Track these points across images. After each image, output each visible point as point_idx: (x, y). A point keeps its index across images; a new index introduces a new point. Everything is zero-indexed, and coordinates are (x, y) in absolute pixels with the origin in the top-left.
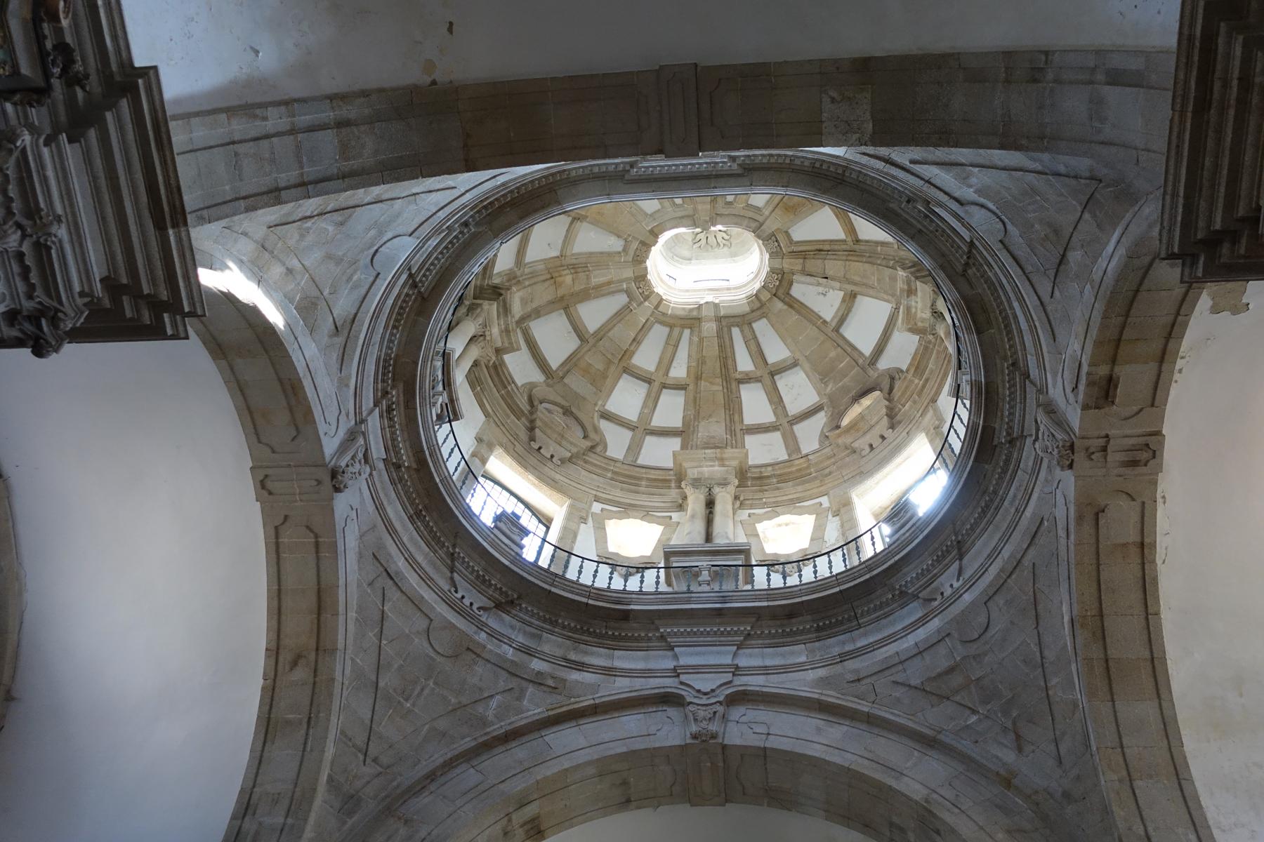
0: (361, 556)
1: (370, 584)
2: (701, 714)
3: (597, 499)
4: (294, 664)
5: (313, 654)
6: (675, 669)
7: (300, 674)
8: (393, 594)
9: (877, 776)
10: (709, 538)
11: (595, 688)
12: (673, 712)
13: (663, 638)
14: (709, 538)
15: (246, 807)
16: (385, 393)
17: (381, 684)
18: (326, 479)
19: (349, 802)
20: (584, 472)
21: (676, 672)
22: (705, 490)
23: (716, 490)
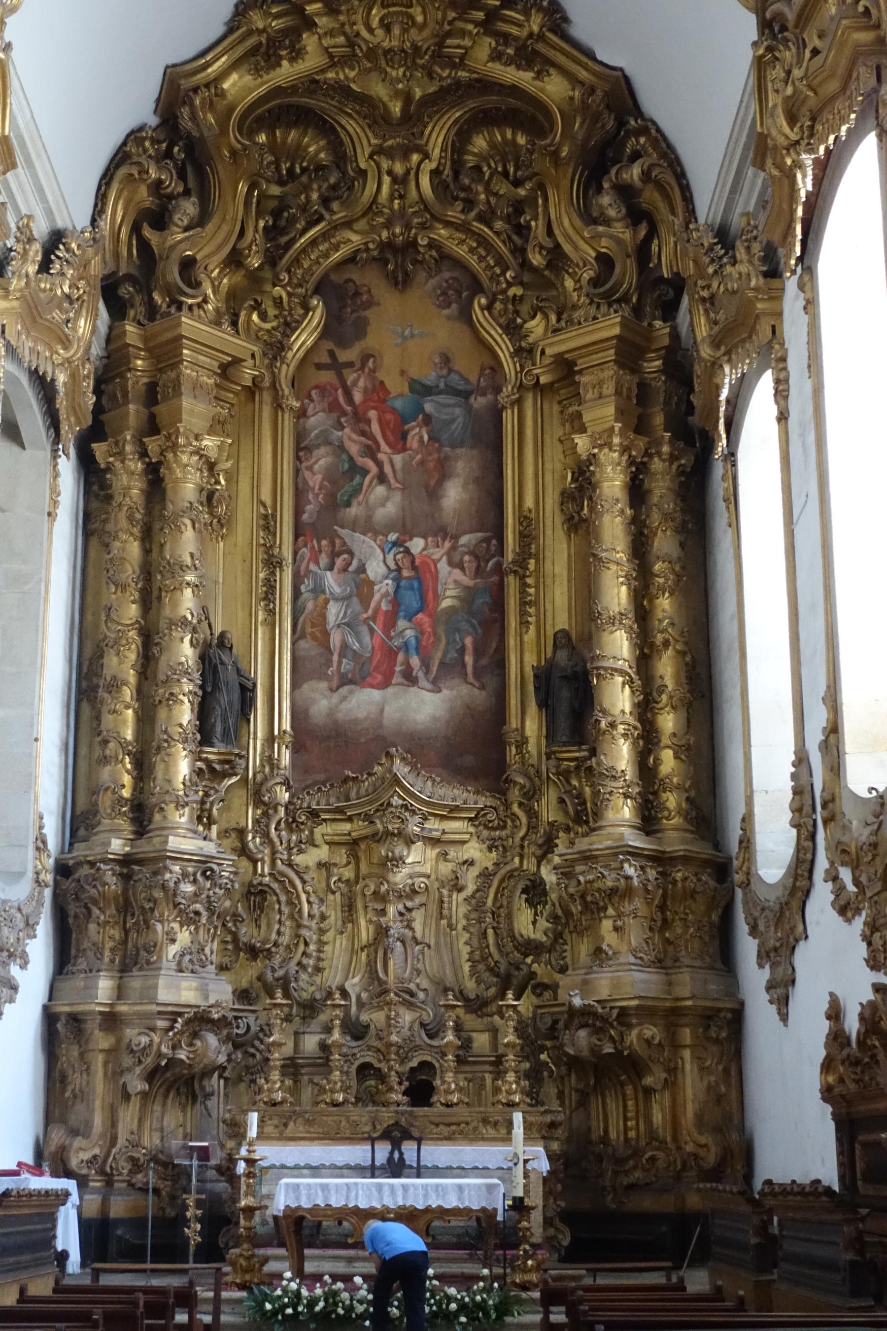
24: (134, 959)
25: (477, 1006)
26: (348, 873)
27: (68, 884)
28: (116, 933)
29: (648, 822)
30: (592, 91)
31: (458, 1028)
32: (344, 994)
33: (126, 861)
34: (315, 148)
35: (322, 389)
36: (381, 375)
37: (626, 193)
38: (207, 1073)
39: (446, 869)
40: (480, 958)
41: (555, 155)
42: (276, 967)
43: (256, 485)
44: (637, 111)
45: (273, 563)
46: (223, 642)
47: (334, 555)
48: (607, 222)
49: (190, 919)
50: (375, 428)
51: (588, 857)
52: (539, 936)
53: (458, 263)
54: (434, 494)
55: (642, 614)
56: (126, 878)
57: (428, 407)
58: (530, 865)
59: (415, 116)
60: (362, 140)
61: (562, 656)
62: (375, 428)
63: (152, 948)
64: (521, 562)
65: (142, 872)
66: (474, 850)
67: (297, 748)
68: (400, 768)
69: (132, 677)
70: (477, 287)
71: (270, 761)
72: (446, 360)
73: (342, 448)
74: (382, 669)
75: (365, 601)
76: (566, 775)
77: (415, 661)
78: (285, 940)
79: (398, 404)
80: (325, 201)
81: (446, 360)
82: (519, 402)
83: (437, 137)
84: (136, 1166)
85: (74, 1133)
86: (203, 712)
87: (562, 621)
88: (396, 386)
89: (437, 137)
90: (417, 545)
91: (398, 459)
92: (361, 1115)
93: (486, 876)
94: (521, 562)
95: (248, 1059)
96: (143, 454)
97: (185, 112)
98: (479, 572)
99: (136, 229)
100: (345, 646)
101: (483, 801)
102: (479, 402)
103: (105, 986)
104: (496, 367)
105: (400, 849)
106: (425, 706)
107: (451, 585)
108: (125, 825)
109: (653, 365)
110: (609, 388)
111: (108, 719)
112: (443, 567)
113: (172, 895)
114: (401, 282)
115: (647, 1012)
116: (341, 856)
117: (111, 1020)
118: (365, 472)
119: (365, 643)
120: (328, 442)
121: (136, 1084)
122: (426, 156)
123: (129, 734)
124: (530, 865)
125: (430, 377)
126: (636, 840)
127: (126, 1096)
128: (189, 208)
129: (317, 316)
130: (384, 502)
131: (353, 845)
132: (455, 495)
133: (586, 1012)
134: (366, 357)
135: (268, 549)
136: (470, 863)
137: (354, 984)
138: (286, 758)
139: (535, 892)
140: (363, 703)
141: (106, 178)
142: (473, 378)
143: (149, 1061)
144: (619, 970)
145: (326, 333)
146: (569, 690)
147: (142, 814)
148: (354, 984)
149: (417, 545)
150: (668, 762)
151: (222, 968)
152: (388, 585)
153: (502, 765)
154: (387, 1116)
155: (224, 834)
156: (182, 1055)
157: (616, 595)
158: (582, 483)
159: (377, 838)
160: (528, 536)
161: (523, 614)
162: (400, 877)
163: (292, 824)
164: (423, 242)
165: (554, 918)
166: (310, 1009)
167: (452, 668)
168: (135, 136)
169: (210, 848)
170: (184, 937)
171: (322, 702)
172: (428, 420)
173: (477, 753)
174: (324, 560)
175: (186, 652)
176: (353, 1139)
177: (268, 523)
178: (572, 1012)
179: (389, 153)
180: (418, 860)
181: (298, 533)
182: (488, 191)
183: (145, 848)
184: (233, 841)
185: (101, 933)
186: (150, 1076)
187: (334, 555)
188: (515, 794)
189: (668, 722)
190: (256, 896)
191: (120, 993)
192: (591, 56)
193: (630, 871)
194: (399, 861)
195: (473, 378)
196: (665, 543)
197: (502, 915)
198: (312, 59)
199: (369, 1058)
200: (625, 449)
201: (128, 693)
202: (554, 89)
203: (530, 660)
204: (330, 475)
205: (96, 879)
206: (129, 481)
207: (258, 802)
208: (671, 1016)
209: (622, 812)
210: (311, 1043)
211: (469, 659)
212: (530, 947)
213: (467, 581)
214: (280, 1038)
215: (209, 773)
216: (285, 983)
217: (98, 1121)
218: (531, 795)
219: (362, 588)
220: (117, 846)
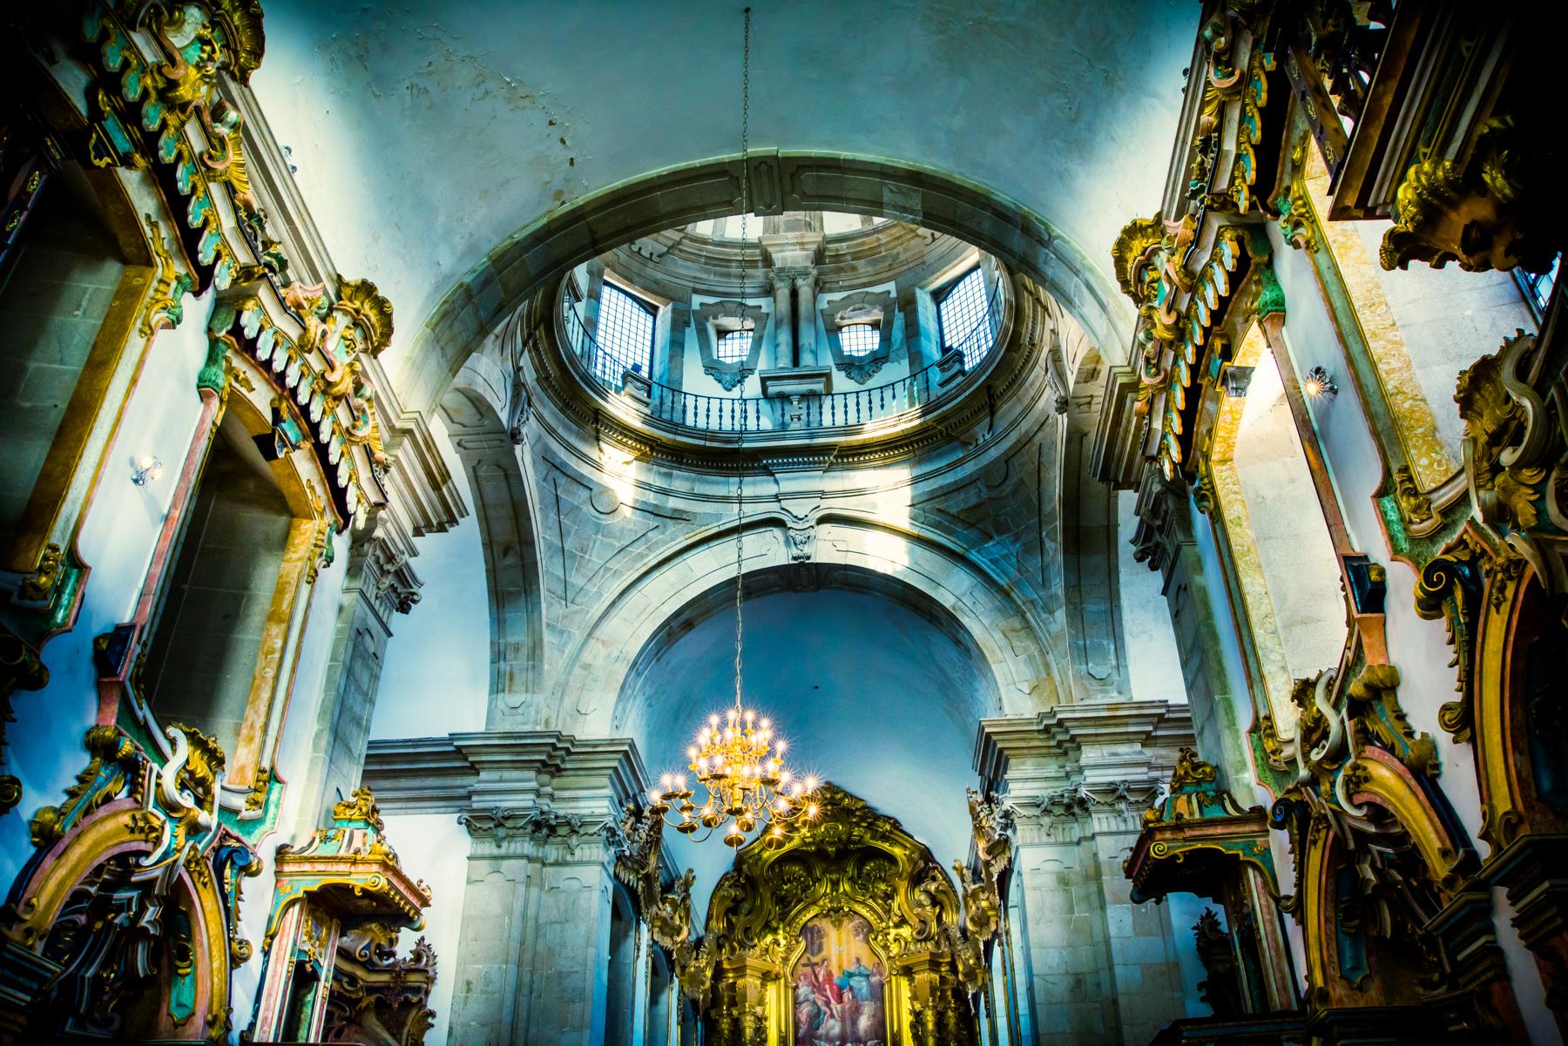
0: (534, 462)
1: (545, 480)
2: (798, 539)
3: (696, 291)
4: (505, 553)
5: (517, 547)
6: (776, 496)
7: (510, 560)
8: (562, 480)
9: (922, 587)
10: (796, 361)
11: (719, 516)
12: (777, 532)
13: (765, 467)
14: (796, 361)
16: (530, 335)
17: (566, 547)
18: (507, 439)
20: (680, 262)
21: (777, 498)
22: (788, 283)
23: (800, 282)
35: (805, 976)
44: (933, 861)
70: (871, 929)
72: (858, 960)
73: (814, 1003)
81: (858, 960)
99: (726, 914)
102: (874, 979)
114: (838, 924)
125: (853, 969)
128: (746, 906)
168: (725, 877)
200: (934, 1007)
204: (809, 1016)
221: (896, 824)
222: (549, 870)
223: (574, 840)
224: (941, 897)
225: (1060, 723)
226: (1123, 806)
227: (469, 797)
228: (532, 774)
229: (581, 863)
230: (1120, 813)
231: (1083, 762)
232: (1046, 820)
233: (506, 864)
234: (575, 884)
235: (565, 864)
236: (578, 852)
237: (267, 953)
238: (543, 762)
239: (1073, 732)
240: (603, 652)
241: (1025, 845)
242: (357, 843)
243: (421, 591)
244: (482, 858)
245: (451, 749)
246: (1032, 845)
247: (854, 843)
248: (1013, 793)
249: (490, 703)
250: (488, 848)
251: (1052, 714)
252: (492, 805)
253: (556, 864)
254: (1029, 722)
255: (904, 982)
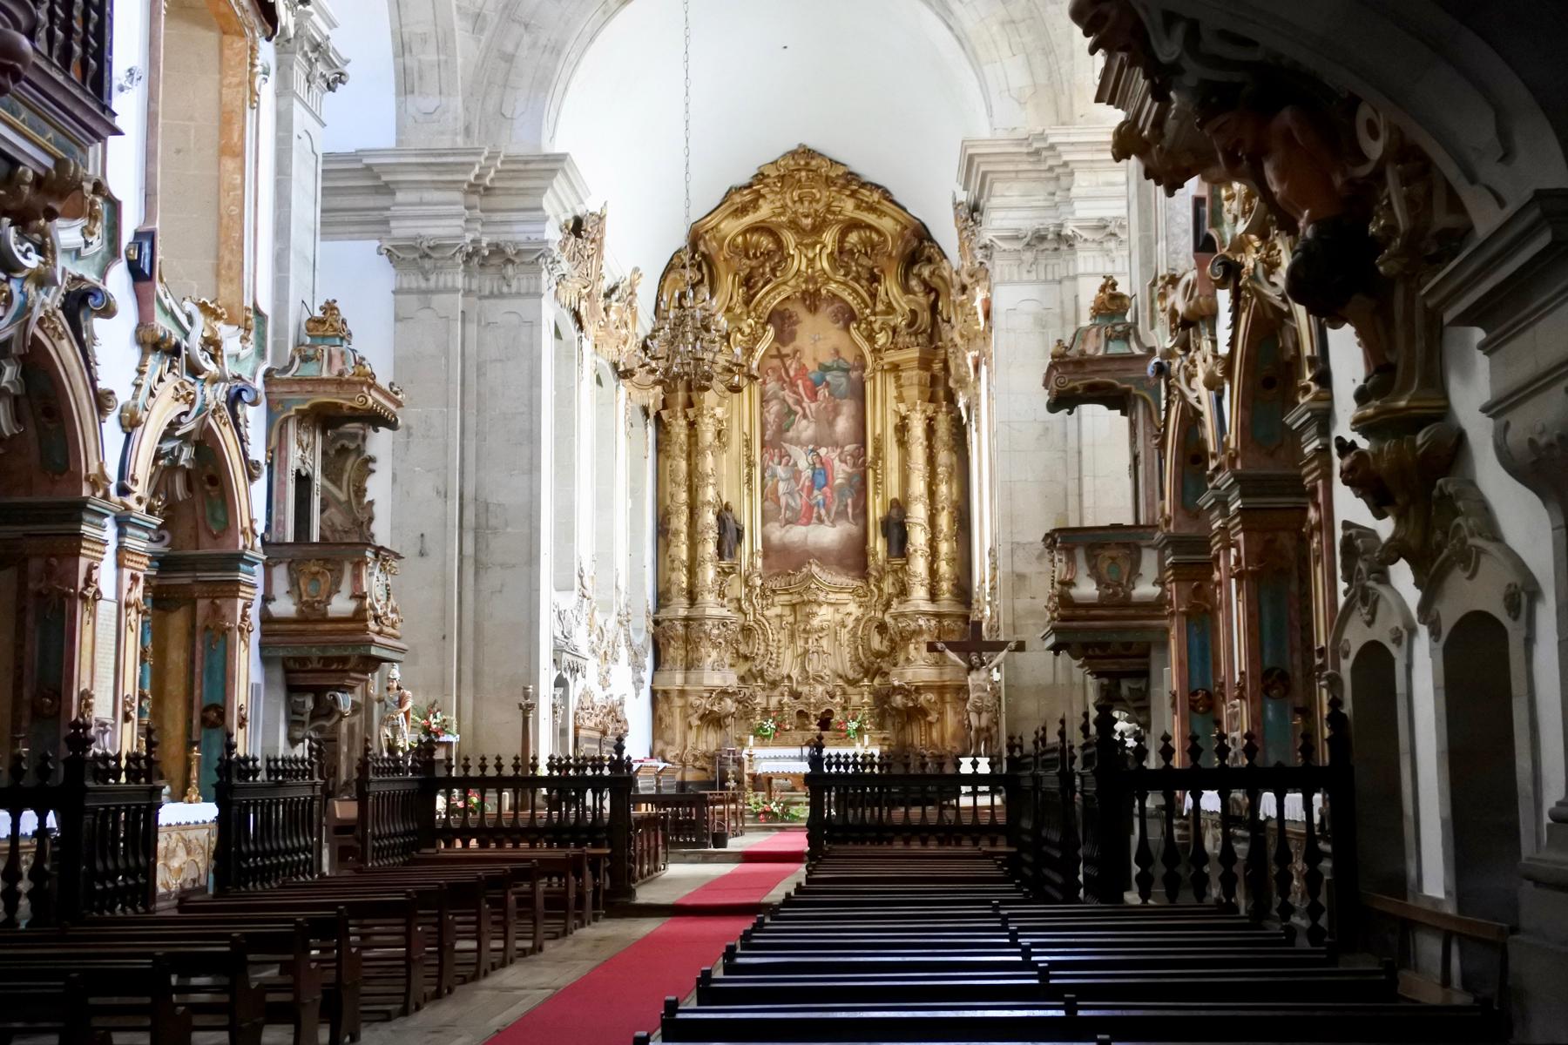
15: (402, 48)
19: (478, 21)
24: (690, 665)
25: (853, 683)
26: (791, 619)
27: (660, 629)
28: (682, 652)
29: (933, 596)
30: (906, 228)
31: (844, 693)
32: (789, 677)
33: (687, 619)
34: (766, 242)
35: (774, 369)
36: (804, 361)
37: (925, 283)
38: (726, 716)
39: (838, 617)
40: (856, 659)
41: (890, 256)
42: (758, 665)
43: (741, 425)
44: (931, 239)
45: (750, 464)
46: (727, 507)
47: (781, 457)
48: (914, 293)
49: (716, 646)
50: (801, 389)
51: (903, 615)
52: (884, 649)
53: (843, 300)
54: (831, 424)
55: (932, 494)
56: (687, 627)
57: (828, 378)
58: (879, 615)
59: (818, 229)
60: (789, 238)
61: (894, 512)
62: (801, 389)
63: (699, 660)
64: (875, 462)
65: (694, 624)
66: (853, 608)
67: (765, 556)
68: (815, 569)
69: (684, 528)
70: (852, 317)
71: (752, 564)
72: (837, 352)
74: (807, 515)
75: (797, 480)
76: (896, 571)
77: (823, 512)
78: (762, 651)
79: (813, 376)
80: (773, 270)
81: (837, 352)
82: (874, 378)
83: (829, 237)
84: (696, 758)
85: (667, 744)
86: (719, 546)
87: (894, 493)
88: (811, 366)
89: (829, 237)
90: (823, 451)
91: (813, 406)
92: (798, 735)
93: (857, 620)
94: (875, 462)
95: (746, 712)
96: (686, 416)
97: (701, 243)
98: (854, 465)
100: (788, 505)
101: (858, 583)
102: (854, 374)
103: (679, 678)
104: (862, 356)
105: (815, 608)
106: (829, 535)
107: (841, 471)
108: (684, 601)
109: (937, 366)
110: (915, 380)
111: (673, 550)
112: (837, 463)
113: (708, 636)
114: (813, 309)
115: (928, 687)
116: (787, 611)
117: (682, 693)
118: (796, 413)
119: (798, 502)
120: (777, 398)
121: (695, 722)
122: (824, 246)
123: (684, 556)
124: (879, 615)
125: (828, 361)
126: (927, 607)
127: (690, 727)
129: (771, 331)
130: (805, 429)
131: (793, 606)
132: (843, 424)
133: (901, 687)
134: (796, 352)
135: (749, 457)
136: (849, 614)
137: (795, 674)
138: (759, 562)
139: (882, 628)
140: (796, 534)
141: (664, 277)
142: (851, 361)
143: (701, 712)
144: (918, 668)
145: (777, 338)
146: (896, 530)
147: (692, 596)
148: (795, 674)
149: (823, 451)
150: (944, 568)
151: (732, 666)
152: (809, 473)
153: (866, 566)
154: (809, 736)
155: (730, 601)
156: (716, 708)
157: (918, 486)
158: (902, 428)
159: (804, 603)
160: (878, 449)
161: (876, 489)
162: (816, 622)
163: (764, 596)
164: (824, 292)
165: (892, 640)
166: (774, 684)
167: (841, 514)
169: (724, 612)
170: (714, 654)
171: (777, 533)
172: (828, 384)
173: (855, 559)
174: (776, 460)
175: (709, 517)
176: (794, 745)
177: (748, 444)
178: (894, 688)
179: (807, 246)
180: (824, 615)
181: (763, 446)
182: (857, 264)
183: (695, 613)
184: (734, 605)
185: (675, 652)
186: (701, 718)
187: (781, 457)
188: (872, 580)
189: (944, 548)
190: (747, 631)
191: (686, 681)
192: (904, 209)
193: (921, 622)
194: (815, 614)
195: (851, 361)
196: (943, 457)
197: (866, 640)
198: (764, 211)
199: (802, 707)
201: (683, 537)
202: (887, 224)
203: (879, 513)
204: (778, 415)
205: (672, 627)
206: (679, 429)
207: (747, 585)
208: (941, 689)
209: (919, 593)
210: (774, 702)
211: (850, 510)
212: (879, 655)
213: (849, 470)
214: (760, 700)
215: (723, 573)
216: (761, 672)
217: (678, 738)
218: (879, 580)
219: (796, 475)
220: (682, 612)
221: (886, 194)
222: (486, 303)
223: (510, 270)
224: (936, 281)
225: (1052, 147)
226: (1112, 244)
227: (386, 222)
228: (457, 196)
229: (518, 294)
230: (1108, 252)
231: (1075, 191)
232: (1028, 256)
233: (437, 300)
234: (514, 318)
235: (501, 295)
236: (514, 284)
237: (270, 466)
238: (471, 185)
239: (1066, 158)
240: (527, 39)
241: (1003, 282)
242: (337, 365)
243: (347, 69)
244: (409, 291)
245: (359, 166)
246: (1011, 282)
247: (834, 213)
248: (996, 224)
249: (398, 108)
250: (415, 281)
251: (1042, 136)
252: (412, 232)
253: (492, 295)
254: (1020, 142)
255: (890, 379)
